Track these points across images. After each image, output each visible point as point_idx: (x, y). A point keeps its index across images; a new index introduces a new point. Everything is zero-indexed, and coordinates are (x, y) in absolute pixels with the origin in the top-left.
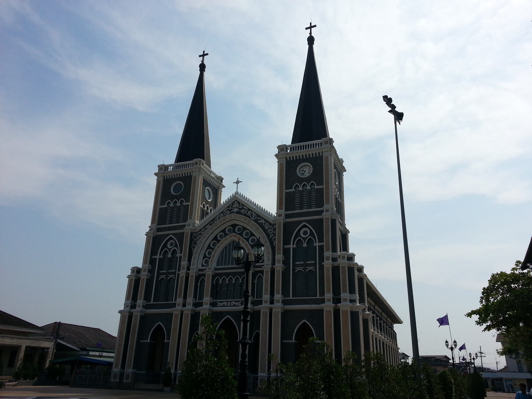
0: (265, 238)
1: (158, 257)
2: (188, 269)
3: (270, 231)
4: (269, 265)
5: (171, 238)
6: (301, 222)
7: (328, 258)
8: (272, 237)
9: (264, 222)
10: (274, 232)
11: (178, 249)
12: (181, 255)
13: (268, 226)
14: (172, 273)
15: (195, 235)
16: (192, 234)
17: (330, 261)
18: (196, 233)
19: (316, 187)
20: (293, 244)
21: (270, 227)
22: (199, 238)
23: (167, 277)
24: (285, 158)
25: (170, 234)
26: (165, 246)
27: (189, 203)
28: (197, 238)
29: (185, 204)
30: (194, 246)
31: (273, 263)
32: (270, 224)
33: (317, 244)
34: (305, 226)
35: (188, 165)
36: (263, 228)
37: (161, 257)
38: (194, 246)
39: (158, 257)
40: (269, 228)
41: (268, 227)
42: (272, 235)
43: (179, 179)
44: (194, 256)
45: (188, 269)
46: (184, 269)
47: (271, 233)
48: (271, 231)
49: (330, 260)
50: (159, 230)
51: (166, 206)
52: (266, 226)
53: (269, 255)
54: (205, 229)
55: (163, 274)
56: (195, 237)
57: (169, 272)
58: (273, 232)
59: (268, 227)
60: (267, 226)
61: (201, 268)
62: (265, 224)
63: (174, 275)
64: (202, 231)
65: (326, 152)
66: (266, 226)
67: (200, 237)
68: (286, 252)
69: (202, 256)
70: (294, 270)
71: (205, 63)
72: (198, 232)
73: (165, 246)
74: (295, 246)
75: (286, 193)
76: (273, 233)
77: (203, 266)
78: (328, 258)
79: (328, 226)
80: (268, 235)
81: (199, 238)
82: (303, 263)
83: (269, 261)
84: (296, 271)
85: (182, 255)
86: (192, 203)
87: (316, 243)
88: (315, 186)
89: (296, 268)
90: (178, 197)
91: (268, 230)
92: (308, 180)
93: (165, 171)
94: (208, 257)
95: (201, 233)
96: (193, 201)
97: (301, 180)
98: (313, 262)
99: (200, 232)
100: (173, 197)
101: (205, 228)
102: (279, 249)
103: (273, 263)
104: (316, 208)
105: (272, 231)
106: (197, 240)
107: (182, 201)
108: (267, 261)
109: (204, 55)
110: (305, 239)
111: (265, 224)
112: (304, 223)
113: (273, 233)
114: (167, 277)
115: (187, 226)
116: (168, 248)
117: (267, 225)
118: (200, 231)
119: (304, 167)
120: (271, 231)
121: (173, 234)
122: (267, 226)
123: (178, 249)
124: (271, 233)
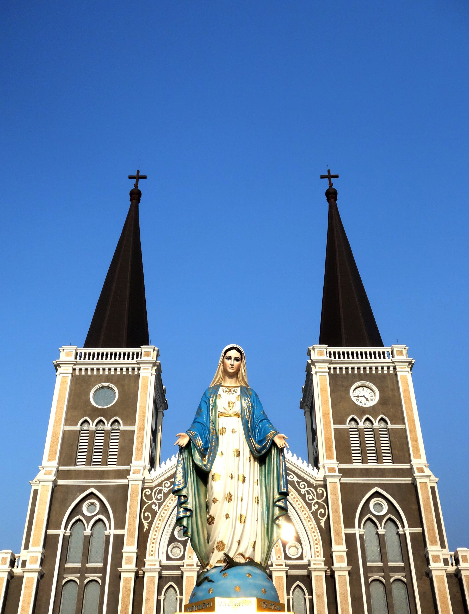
0: (306, 511)
1: (61, 532)
2: (140, 561)
3: (311, 498)
4: (320, 564)
5: (92, 495)
6: (370, 486)
7: (436, 559)
8: (317, 510)
9: (296, 479)
10: (319, 501)
11: (108, 518)
12: (119, 532)
13: (306, 489)
14: (94, 571)
15: (148, 493)
16: (143, 489)
17: (441, 564)
18: (151, 488)
19: (390, 426)
20: (359, 527)
21: (310, 490)
22: (157, 499)
23: (82, 578)
24: (327, 368)
25: (89, 487)
26: (77, 509)
27: (135, 428)
28: (154, 500)
29: (122, 428)
30: (146, 515)
31: (329, 561)
32: (310, 485)
33: (408, 531)
34: (376, 494)
35: (140, 354)
36: (298, 491)
37: (68, 533)
38: (146, 515)
39: (61, 532)
40: (309, 493)
41: (307, 491)
42: (317, 506)
43: (109, 379)
44: (152, 537)
45: (140, 561)
46: (128, 562)
47: (314, 502)
48: (313, 499)
49: (440, 562)
50: (60, 474)
51: (78, 428)
52: (301, 488)
53: (317, 544)
54: (170, 481)
55: (73, 571)
56: (149, 497)
57: (87, 568)
58: (316, 500)
59: (307, 491)
60: (304, 488)
61: (165, 563)
62: (298, 483)
63: (100, 575)
64: (165, 487)
65: (401, 368)
66: (301, 488)
67: (159, 497)
68: (350, 539)
69: (166, 538)
70: (366, 578)
71: (139, 188)
72: (156, 487)
73: (77, 509)
74: (362, 531)
75: (335, 430)
76: (317, 502)
77: (168, 558)
78: (436, 559)
79: (428, 498)
80: (309, 506)
81: (157, 499)
82: (380, 564)
83: (318, 556)
84: (370, 580)
85: (125, 532)
86: (142, 429)
87: (403, 527)
88: (387, 423)
89: (369, 574)
90: (107, 413)
91: (307, 496)
92: (373, 411)
93: (76, 358)
94: (180, 541)
95: (160, 492)
96: (143, 425)
97: (362, 411)
98: (402, 564)
99: (160, 488)
100: (95, 413)
101: (171, 480)
102: (338, 533)
103: (329, 561)
104: (393, 463)
105: (315, 498)
106: (154, 503)
107: (116, 421)
108: (315, 557)
109: (138, 177)
110: (380, 518)
111: (298, 483)
112: (376, 489)
113: (317, 503)
114: (82, 578)
115: (134, 473)
116: (83, 515)
117: (303, 486)
118: (160, 485)
119: (361, 389)
120: (313, 499)
121: (99, 488)
122: (304, 488)
123: (108, 518)
124: (314, 502)
